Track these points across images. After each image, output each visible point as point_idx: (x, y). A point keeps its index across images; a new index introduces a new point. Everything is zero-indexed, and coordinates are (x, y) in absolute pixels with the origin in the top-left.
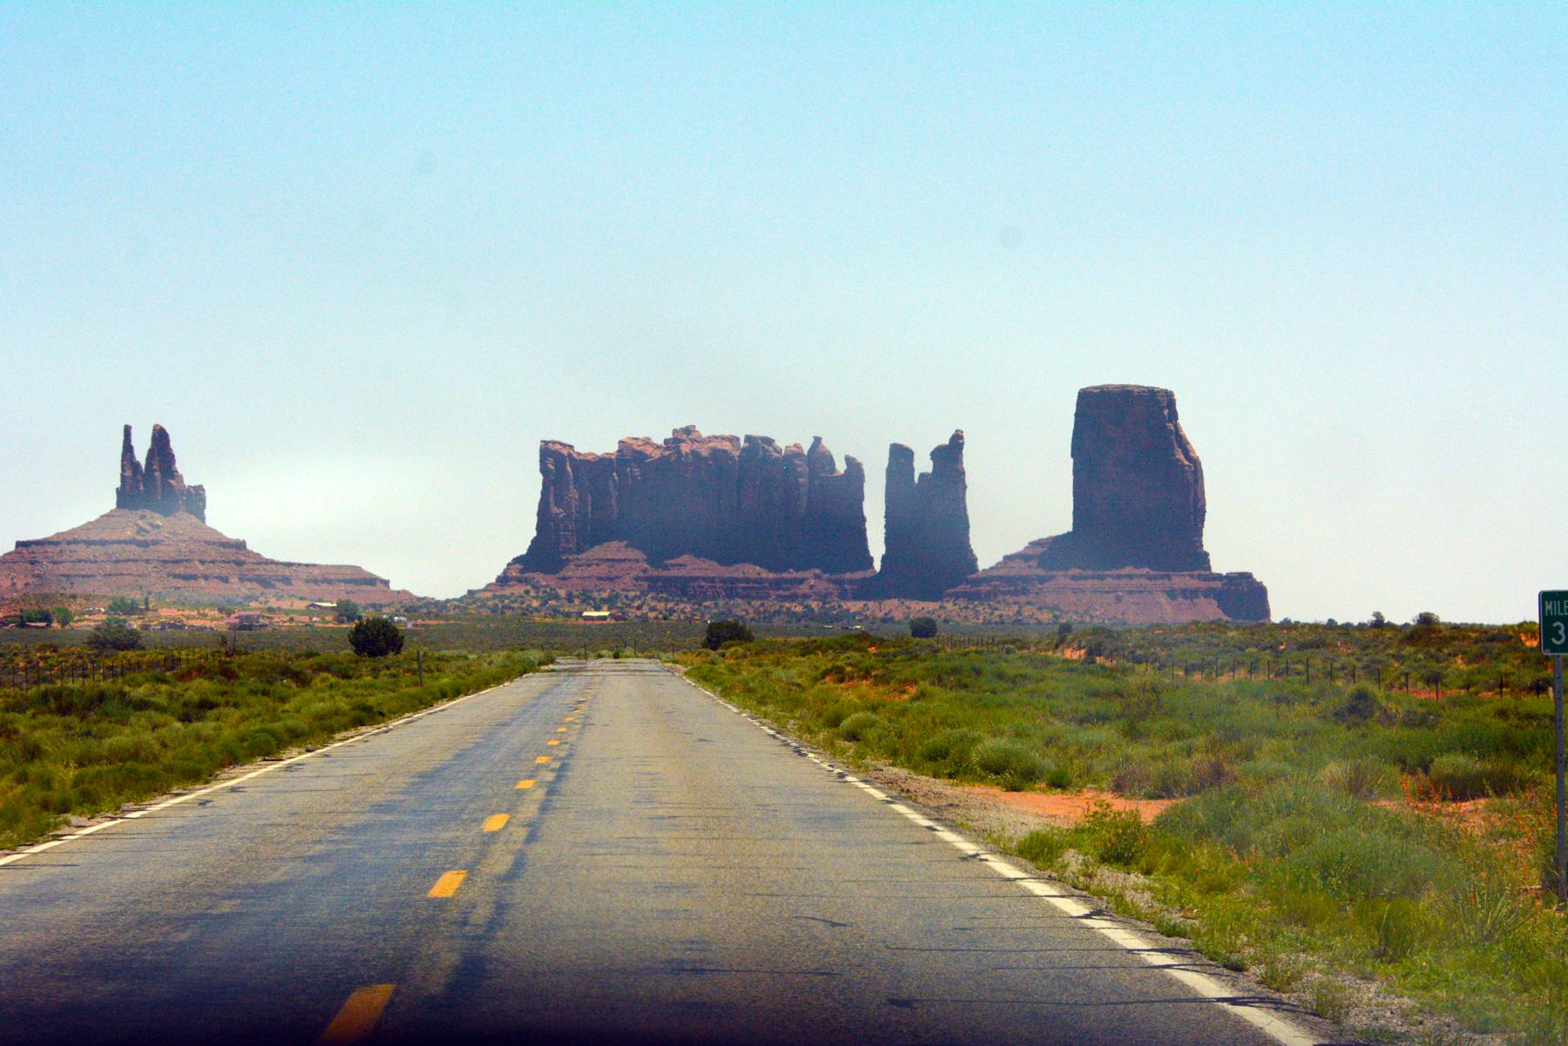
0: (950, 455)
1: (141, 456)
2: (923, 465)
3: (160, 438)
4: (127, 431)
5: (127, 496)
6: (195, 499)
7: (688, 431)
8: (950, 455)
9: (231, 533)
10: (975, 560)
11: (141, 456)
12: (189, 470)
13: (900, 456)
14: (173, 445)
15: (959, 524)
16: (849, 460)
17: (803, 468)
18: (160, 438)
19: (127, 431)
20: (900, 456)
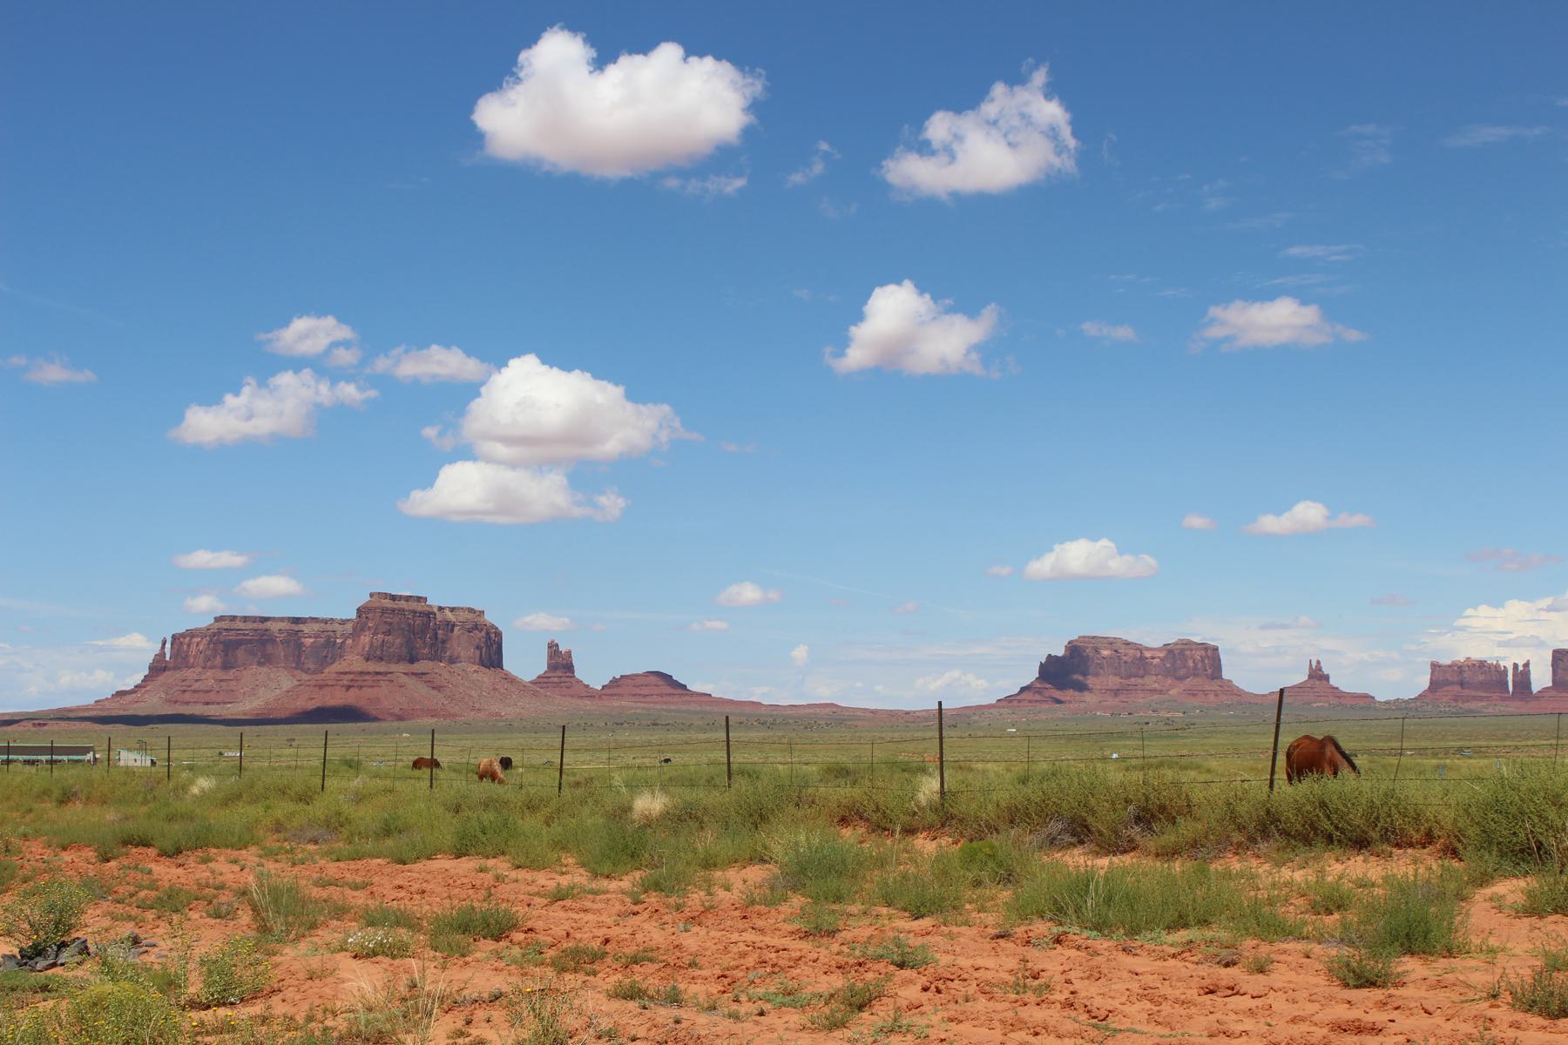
0: (1527, 665)
1: (1314, 667)
2: (1521, 668)
3: (1318, 662)
4: (1310, 661)
5: (1310, 677)
6: (1327, 678)
7: (1469, 658)
8: (1527, 665)
9: (1336, 686)
10: (1531, 692)
11: (1314, 667)
12: (1326, 671)
13: (1516, 666)
14: (1322, 664)
15: (1529, 683)
16: (1505, 667)
17: (1493, 668)
18: (1318, 662)
19: (1310, 661)
20: (1516, 666)
